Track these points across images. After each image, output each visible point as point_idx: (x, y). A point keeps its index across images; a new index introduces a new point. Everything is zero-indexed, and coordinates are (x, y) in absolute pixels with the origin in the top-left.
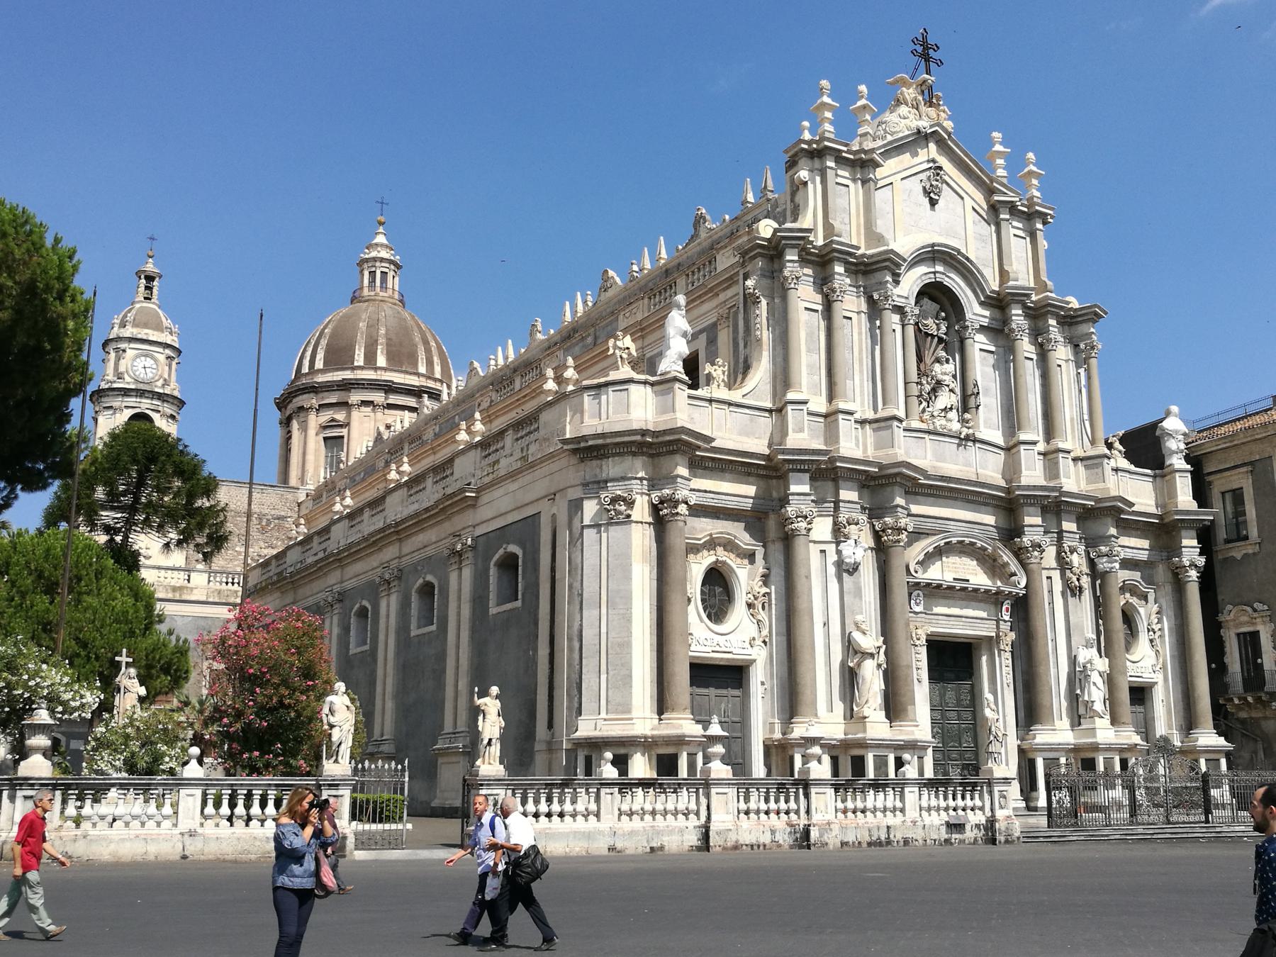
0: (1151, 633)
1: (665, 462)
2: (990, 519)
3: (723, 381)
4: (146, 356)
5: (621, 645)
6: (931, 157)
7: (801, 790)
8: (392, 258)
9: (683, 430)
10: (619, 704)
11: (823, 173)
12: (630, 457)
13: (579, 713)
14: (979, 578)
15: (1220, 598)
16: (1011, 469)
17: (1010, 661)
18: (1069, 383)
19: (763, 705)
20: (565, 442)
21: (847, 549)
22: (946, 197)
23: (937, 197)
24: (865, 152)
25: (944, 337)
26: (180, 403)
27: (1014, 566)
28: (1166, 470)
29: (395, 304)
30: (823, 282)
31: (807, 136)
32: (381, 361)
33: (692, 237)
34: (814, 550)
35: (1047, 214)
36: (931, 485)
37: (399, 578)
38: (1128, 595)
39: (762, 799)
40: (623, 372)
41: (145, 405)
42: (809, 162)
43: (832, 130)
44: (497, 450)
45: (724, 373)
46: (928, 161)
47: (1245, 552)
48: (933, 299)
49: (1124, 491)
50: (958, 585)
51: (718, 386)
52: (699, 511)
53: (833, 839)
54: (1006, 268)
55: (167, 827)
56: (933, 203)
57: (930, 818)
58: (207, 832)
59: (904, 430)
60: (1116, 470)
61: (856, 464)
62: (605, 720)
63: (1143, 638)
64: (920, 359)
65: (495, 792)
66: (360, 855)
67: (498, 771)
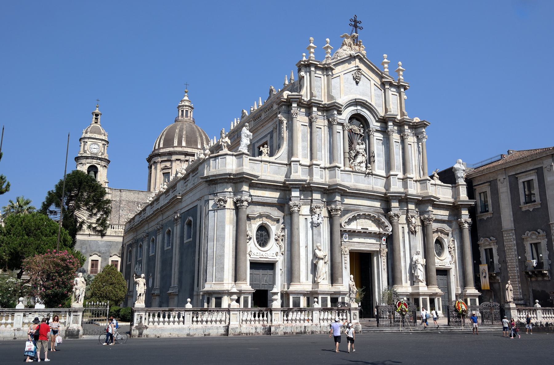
0: (450, 249)
1: (239, 185)
2: (377, 204)
3: (267, 153)
4: (95, 144)
5: (220, 256)
6: (357, 65)
7: (269, 313)
8: (190, 105)
9: (244, 173)
10: (219, 278)
12: (226, 184)
13: (206, 281)
14: (373, 228)
15: (479, 235)
16: (387, 186)
17: (385, 260)
18: (414, 151)
19: (281, 278)
20: (202, 178)
21: (315, 218)
22: (363, 80)
23: (359, 81)
24: (327, 64)
25: (363, 134)
26: (108, 162)
27: (387, 223)
28: (457, 185)
29: (191, 122)
30: (309, 114)
31: (304, 59)
32: (184, 144)
33: (269, 97)
34: (302, 219)
35: (405, 86)
36: (353, 192)
37: (162, 228)
38: (439, 233)
39: (253, 316)
40: (225, 151)
41: (94, 162)
42: (305, 68)
43: (314, 56)
44: (188, 181)
45: (268, 150)
46: (355, 67)
47: (487, 217)
48: (358, 120)
49: (438, 193)
50: (362, 231)
51: (265, 155)
52: (252, 203)
53: (280, 332)
54: (387, 107)
55: (9, 327)
56: (357, 83)
57: (323, 323)
58: (24, 329)
59: (341, 171)
60: (435, 185)
61: (319, 185)
62: (214, 284)
63: (446, 250)
64: (351, 143)
65: (141, 313)
66: (85, 337)
67: (142, 306)
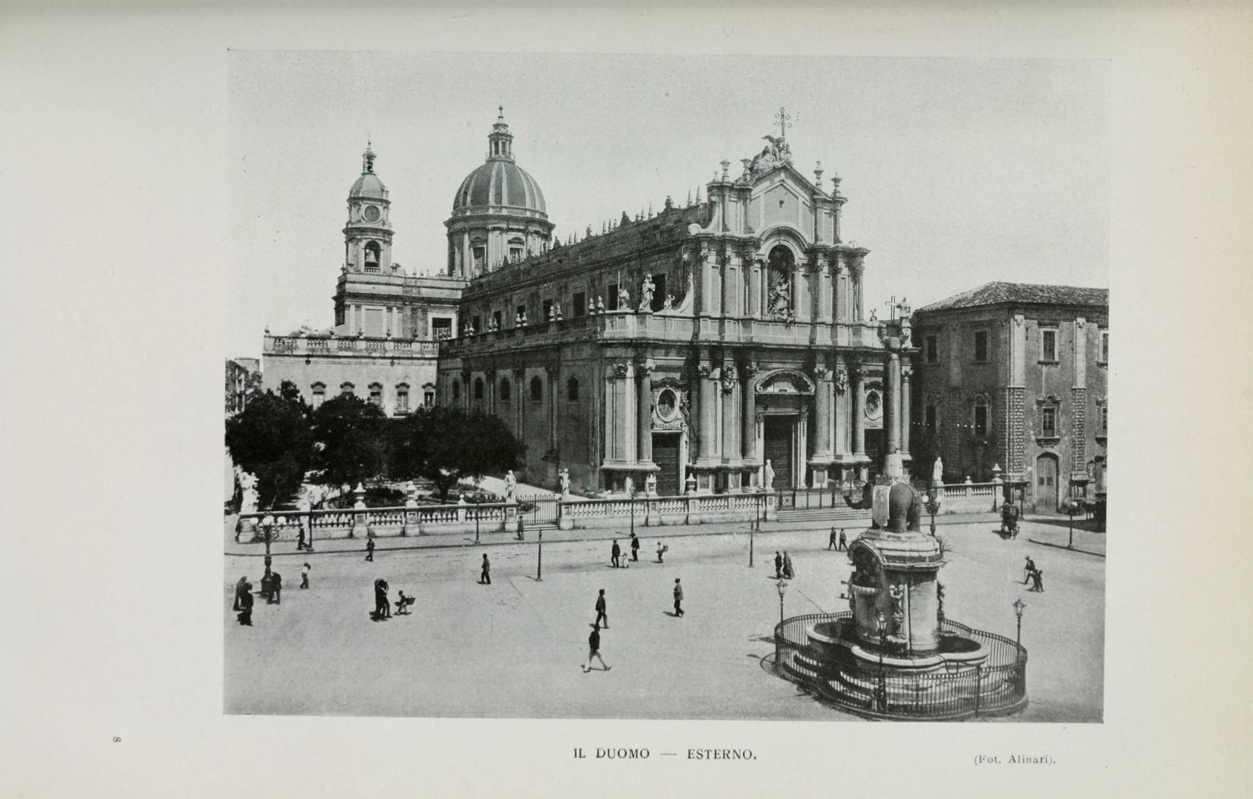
11: (724, 196)
14: (791, 390)
